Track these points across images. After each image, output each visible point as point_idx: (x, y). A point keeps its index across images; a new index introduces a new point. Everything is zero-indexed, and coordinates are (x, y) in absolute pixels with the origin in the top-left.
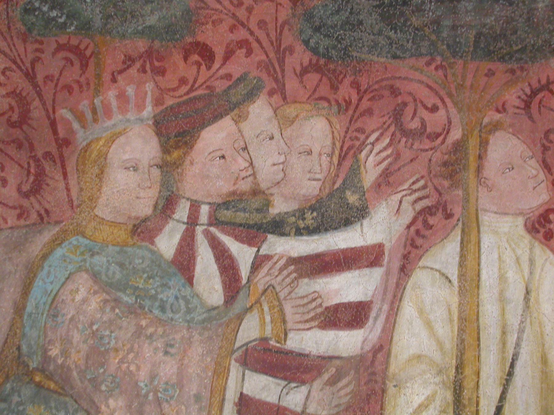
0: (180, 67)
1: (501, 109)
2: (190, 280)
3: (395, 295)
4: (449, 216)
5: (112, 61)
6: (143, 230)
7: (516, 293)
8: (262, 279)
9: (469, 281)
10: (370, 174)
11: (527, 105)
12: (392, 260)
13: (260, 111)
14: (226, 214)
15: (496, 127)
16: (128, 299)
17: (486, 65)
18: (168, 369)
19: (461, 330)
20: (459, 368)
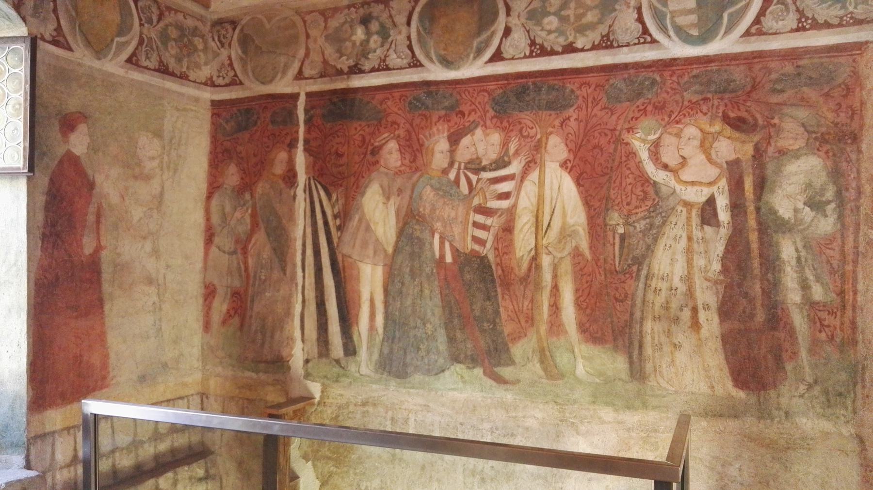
0: (455, 119)
1: (554, 127)
2: (458, 187)
3: (519, 189)
4: (536, 163)
5: (435, 118)
6: (445, 172)
7: (556, 187)
8: (479, 186)
9: (541, 184)
10: (512, 151)
11: (562, 126)
12: (518, 178)
13: (479, 132)
14: (469, 166)
15: (551, 133)
16: (441, 193)
17: (549, 112)
18: (453, 214)
19: (539, 199)
20: (538, 211)
